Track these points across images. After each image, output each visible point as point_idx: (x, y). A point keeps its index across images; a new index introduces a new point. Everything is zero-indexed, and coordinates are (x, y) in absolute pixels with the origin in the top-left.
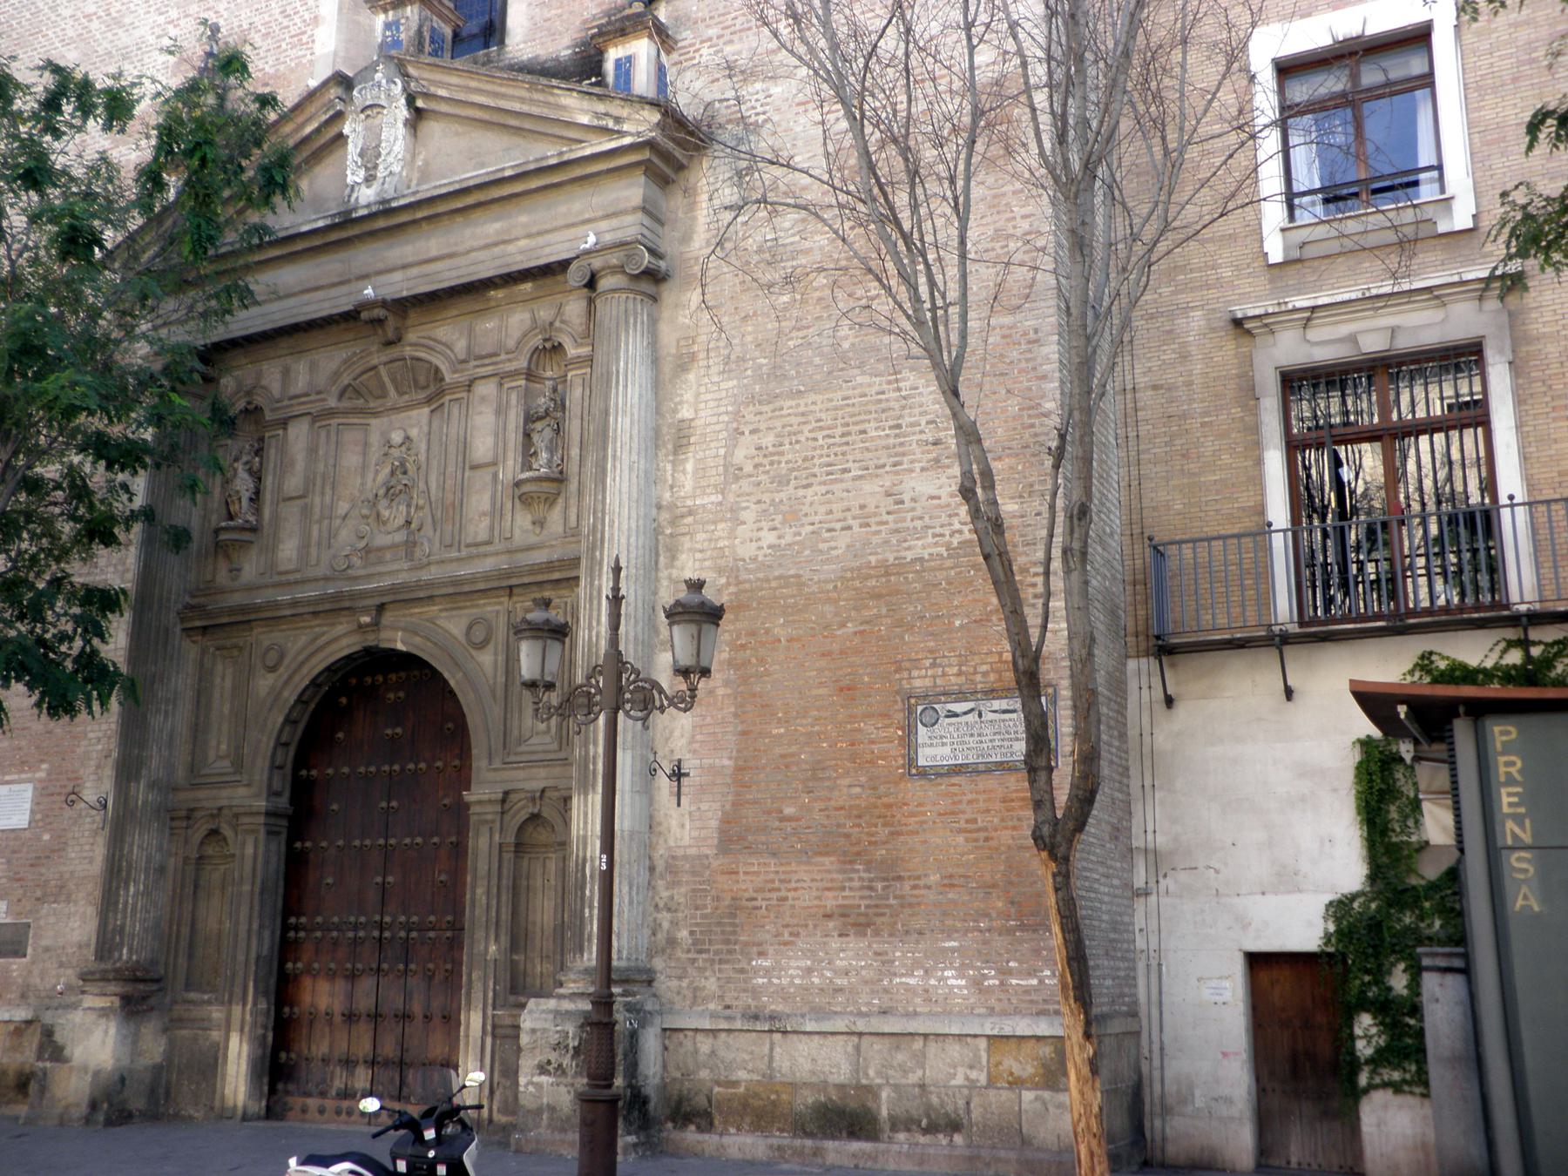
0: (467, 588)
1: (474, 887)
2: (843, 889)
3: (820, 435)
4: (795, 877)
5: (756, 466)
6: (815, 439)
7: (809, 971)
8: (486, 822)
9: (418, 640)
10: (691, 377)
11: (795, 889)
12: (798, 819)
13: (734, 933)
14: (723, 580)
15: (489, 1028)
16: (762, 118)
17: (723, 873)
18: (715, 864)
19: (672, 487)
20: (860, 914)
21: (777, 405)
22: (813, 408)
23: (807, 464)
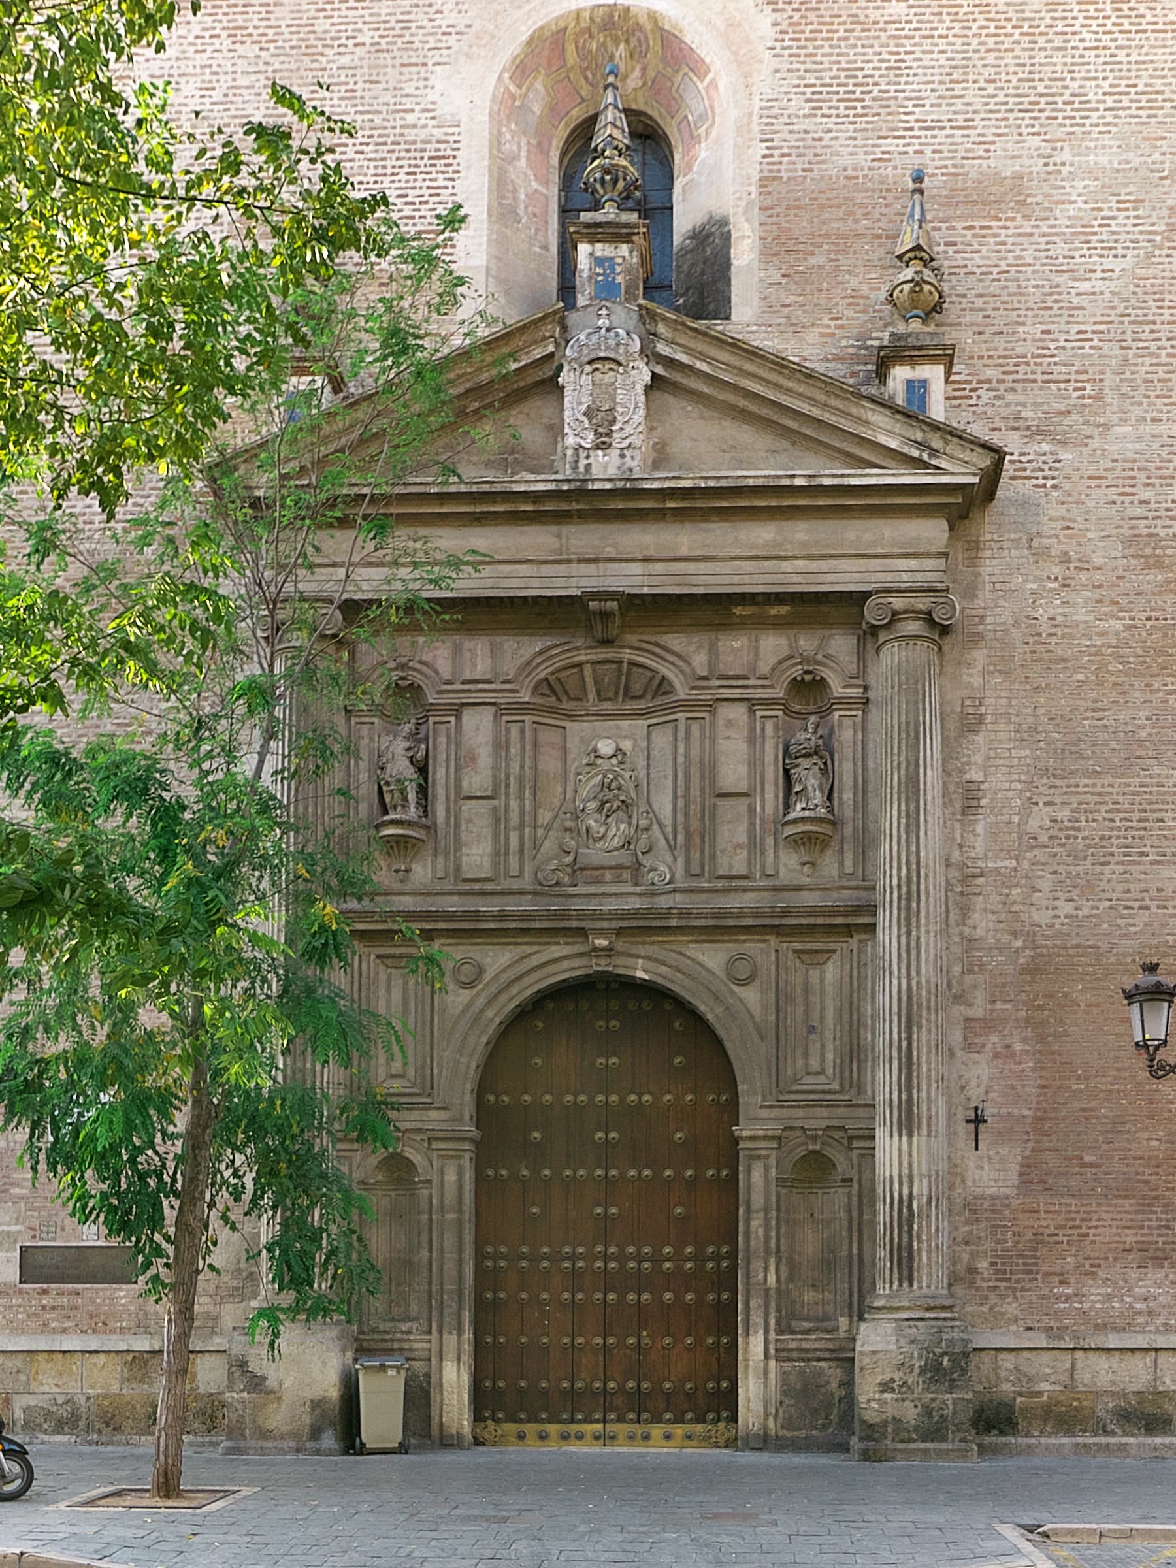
0: (731, 922)
1: (748, 1221)
2: (1142, 1227)
3: (1117, 817)
4: (1095, 1217)
5: (1051, 838)
6: (1113, 820)
7: (1109, 1298)
8: (759, 1157)
9: (664, 969)
10: (980, 739)
11: (1096, 1227)
12: (1098, 1166)
13: (1036, 1264)
14: (1019, 943)
15: (772, 1352)
16: (1049, 483)
17: (1024, 1211)
18: (1015, 1203)
19: (961, 846)
20: (1158, 1249)
21: (1072, 781)
22: (1110, 789)
23: (1104, 843)
